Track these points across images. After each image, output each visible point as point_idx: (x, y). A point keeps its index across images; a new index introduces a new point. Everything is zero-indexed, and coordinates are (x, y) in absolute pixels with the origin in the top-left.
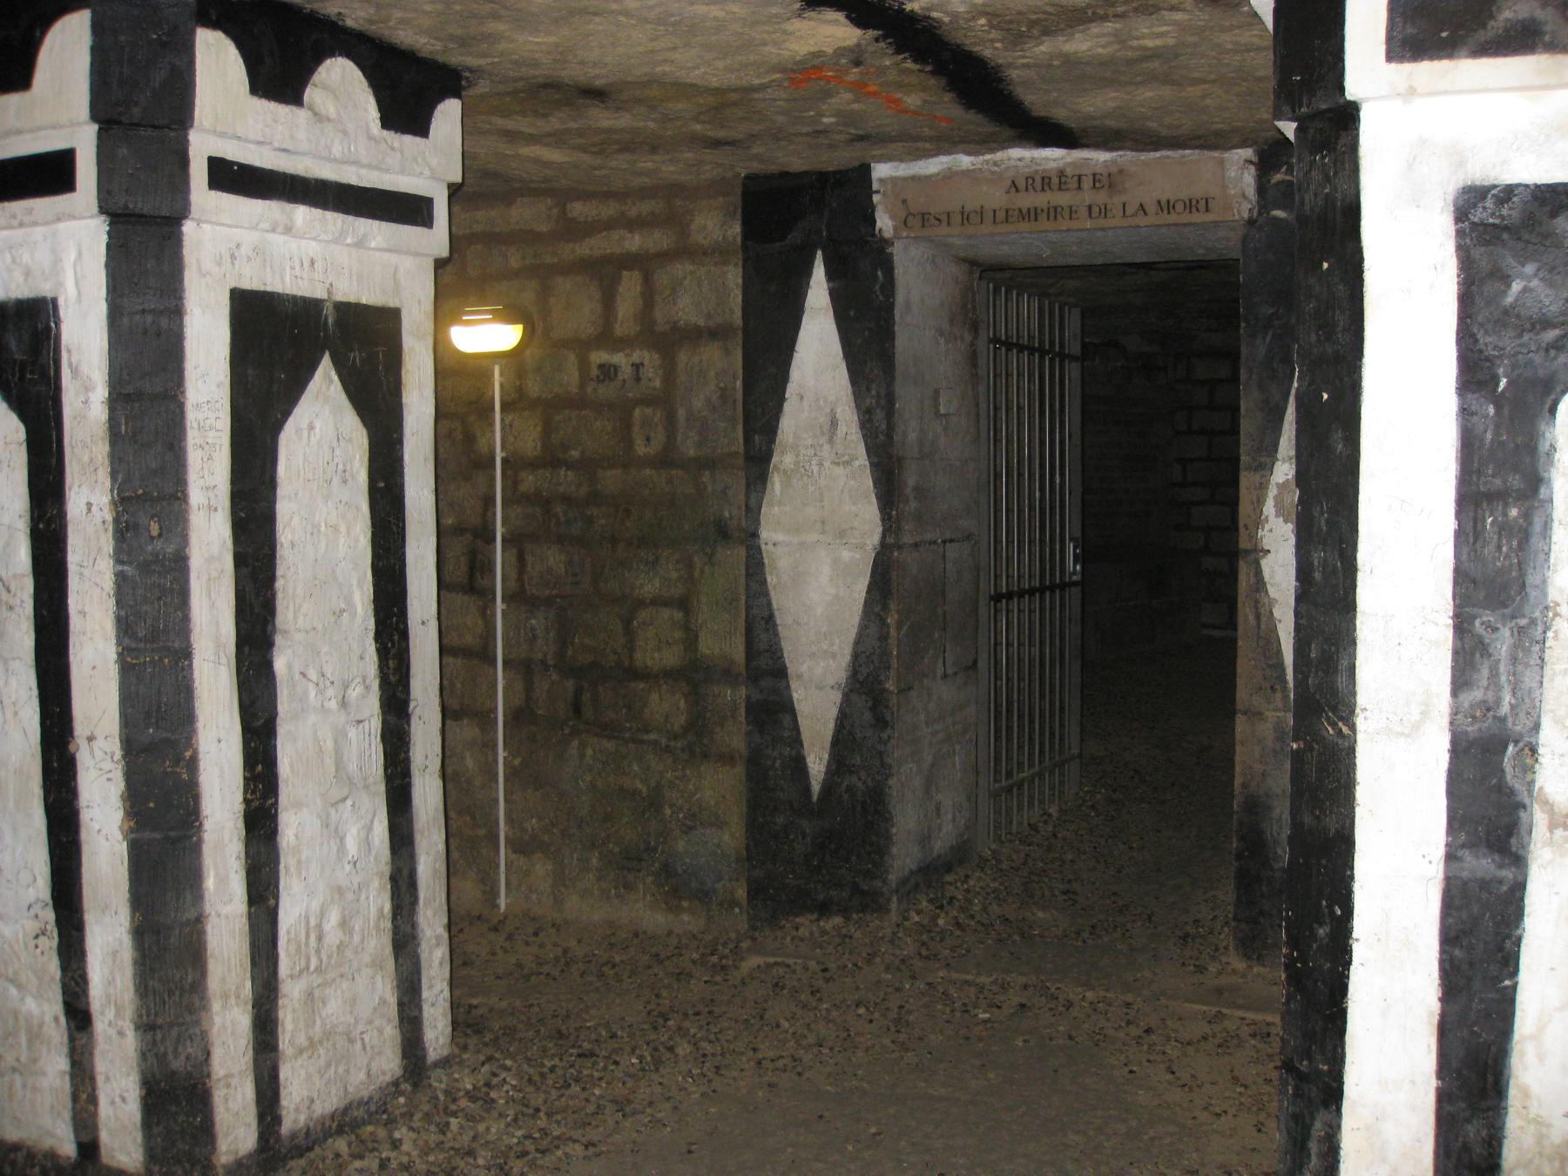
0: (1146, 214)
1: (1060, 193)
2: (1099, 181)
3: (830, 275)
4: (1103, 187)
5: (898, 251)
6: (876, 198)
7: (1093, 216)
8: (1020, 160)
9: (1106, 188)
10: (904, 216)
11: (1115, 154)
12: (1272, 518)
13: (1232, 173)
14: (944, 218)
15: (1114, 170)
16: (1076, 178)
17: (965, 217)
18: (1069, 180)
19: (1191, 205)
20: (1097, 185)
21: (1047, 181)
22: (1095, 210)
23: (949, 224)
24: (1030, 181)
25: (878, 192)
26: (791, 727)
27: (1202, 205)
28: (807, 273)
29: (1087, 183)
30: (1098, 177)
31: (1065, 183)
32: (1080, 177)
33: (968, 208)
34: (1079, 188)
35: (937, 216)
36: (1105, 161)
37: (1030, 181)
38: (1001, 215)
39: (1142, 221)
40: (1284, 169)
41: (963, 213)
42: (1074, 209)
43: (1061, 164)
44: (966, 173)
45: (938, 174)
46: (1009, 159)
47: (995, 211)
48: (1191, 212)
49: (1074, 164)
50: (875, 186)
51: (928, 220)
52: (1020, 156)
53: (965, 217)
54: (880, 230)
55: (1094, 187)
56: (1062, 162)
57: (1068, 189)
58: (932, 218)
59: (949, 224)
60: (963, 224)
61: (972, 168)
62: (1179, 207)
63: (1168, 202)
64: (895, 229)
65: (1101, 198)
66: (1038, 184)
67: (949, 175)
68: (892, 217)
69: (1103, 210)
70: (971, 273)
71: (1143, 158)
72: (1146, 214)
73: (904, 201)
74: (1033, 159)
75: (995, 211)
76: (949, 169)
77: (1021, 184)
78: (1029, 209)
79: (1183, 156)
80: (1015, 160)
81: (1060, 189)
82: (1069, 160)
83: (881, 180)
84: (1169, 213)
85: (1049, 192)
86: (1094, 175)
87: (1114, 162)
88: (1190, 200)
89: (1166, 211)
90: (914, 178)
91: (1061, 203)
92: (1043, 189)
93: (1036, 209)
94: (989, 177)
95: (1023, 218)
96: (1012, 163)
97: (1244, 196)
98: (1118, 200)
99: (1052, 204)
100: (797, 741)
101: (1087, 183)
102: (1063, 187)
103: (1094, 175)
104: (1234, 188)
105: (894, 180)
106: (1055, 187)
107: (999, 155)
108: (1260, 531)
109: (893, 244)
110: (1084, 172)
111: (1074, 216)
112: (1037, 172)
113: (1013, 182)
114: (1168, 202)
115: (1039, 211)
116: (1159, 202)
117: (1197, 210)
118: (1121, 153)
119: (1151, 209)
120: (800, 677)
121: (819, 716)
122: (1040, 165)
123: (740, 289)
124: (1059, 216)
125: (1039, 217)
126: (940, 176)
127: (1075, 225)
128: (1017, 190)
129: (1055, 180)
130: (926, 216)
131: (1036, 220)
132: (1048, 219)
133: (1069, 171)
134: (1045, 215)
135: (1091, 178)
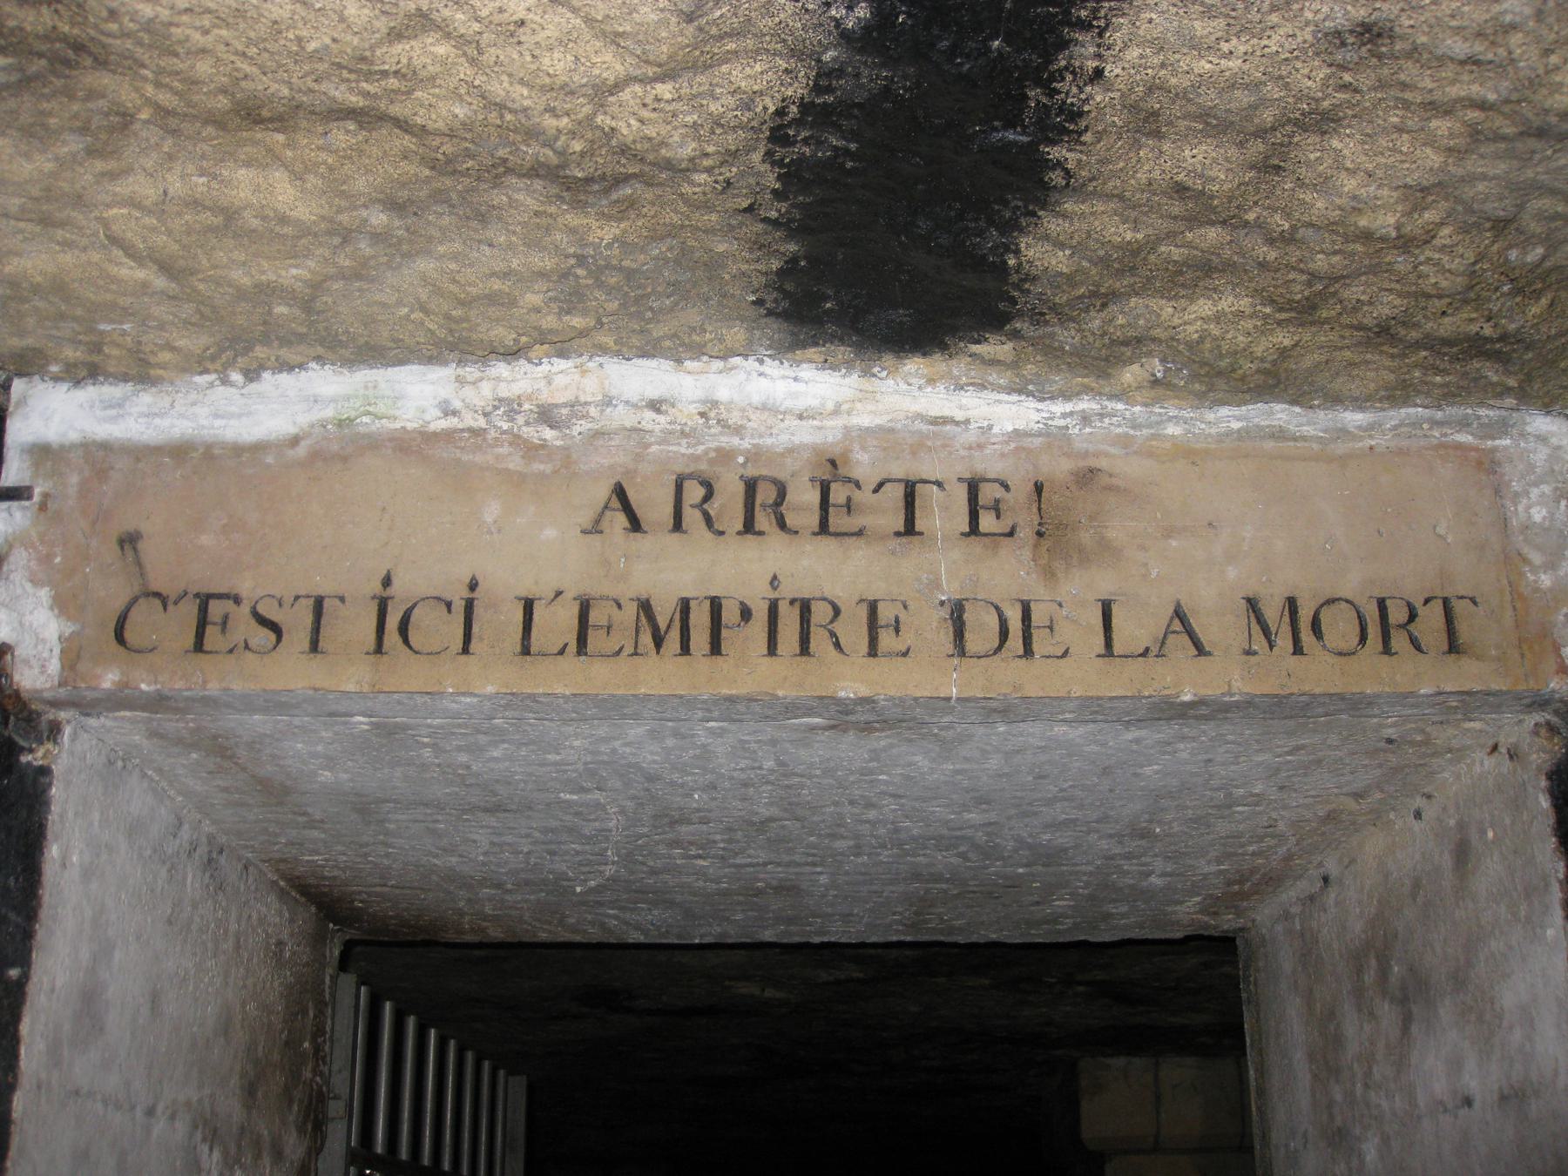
0: (1200, 650)
1: (827, 544)
7: (973, 643)
8: (655, 406)
9: (1025, 533)
10: (119, 604)
11: (1059, 407)
14: (298, 622)
15: (1058, 468)
16: (895, 493)
18: (858, 496)
20: (987, 522)
21: (765, 494)
22: (981, 629)
23: (314, 647)
24: (694, 493)
27: (1431, 622)
30: (988, 493)
31: (849, 506)
34: (910, 529)
37: (694, 493)
38: (556, 623)
42: (886, 614)
43: (828, 434)
45: (295, 441)
46: (608, 401)
47: (528, 606)
48: (1387, 650)
49: (885, 437)
52: (653, 393)
53: (393, 622)
55: (974, 529)
56: (838, 422)
57: (859, 533)
58: (245, 609)
60: (379, 649)
62: (1340, 629)
63: (1292, 604)
64: (72, 654)
68: (62, 605)
70: (319, 939)
71: (1172, 430)
72: (1200, 650)
73: (129, 541)
74: (709, 409)
75: (528, 606)
77: (655, 503)
78: (685, 606)
79: (1343, 433)
81: (824, 528)
82: (864, 419)
83: (42, 453)
84: (1298, 650)
85: (776, 539)
86: (973, 487)
87: (1054, 438)
88: (1382, 604)
89: (1284, 642)
90: (179, 451)
92: (749, 527)
94: (515, 463)
95: (658, 641)
96: (621, 417)
99: (787, 591)
102: (837, 521)
109: (55, 730)
110: (927, 468)
111: (886, 640)
112: (725, 456)
113: (620, 492)
114: (1292, 604)
115: (730, 614)
116: (1252, 604)
117: (1416, 644)
118: (1086, 404)
122: (738, 430)
124: (819, 640)
126: (301, 451)
128: (635, 524)
129: (805, 496)
130: (216, 609)
131: (716, 648)
133: (864, 465)
134: (758, 627)
135: (962, 493)
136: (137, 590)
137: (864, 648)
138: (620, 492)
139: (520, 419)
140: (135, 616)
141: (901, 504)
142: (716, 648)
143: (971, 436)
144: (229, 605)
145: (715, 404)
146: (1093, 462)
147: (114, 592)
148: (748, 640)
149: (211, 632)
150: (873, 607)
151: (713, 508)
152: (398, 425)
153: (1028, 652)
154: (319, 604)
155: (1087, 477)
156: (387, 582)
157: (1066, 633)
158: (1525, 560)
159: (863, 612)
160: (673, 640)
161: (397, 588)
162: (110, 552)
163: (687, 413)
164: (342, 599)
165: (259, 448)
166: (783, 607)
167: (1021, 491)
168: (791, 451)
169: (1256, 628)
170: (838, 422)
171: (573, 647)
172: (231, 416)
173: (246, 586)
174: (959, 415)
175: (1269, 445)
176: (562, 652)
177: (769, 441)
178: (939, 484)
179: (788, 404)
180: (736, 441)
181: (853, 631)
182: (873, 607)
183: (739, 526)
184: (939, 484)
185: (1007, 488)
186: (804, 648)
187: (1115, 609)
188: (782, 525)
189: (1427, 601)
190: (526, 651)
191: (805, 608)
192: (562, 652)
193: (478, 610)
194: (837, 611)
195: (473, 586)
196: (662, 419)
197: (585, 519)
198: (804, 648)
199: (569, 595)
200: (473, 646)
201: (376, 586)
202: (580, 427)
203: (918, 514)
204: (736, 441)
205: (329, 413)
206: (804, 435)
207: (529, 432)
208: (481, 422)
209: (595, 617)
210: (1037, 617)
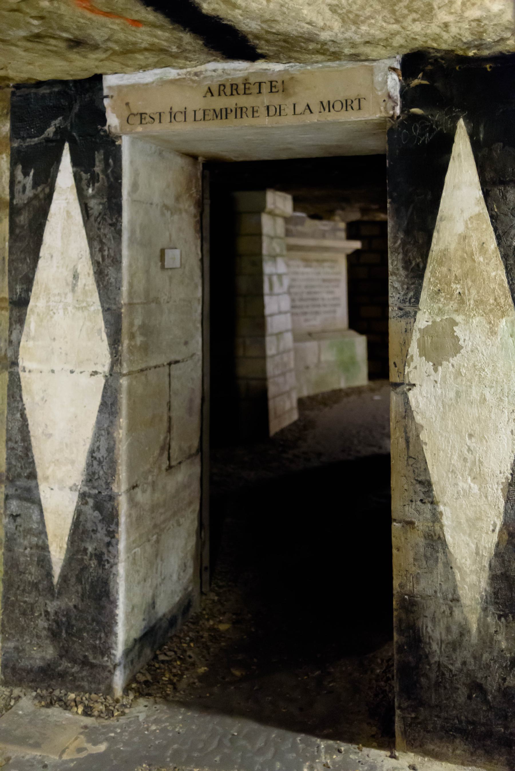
0: (311, 112)
1: (245, 96)
2: (275, 87)
3: (75, 162)
5: (125, 143)
6: (106, 102)
7: (270, 114)
8: (214, 71)
9: (281, 91)
12: (416, 358)
13: (379, 78)
14: (157, 117)
15: (287, 77)
16: (257, 85)
17: (173, 116)
18: (251, 86)
21: (234, 87)
23: (160, 122)
24: (222, 88)
26: (39, 520)
28: (58, 160)
29: (265, 89)
30: (274, 84)
32: (260, 83)
33: (175, 110)
34: (260, 92)
35: (152, 116)
36: (280, 71)
37: (222, 88)
40: (420, 75)
41: (171, 113)
42: (255, 109)
44: (173, 82)
45: (153, 83)
47: (195, 111)
48: (347, 110)
50: (106, 92)
51: (145, 118)
52: (214, 68)
53: (173, 116)
55: (271, 92)
56: (247, 71)
57: (251, 94)
59: (160, 122)
60: (171, 122)
61: (178, 77)
62: (338, 106)
63: (329, 102)
65: (276, 100)
66: (228, 90)
67: (163, 83)
68: (118, 117)
72: (311, 112)
73: (127, 104)
74: (224, 70)
75: (195, 111)
76: (161, 78)
77: (215, 90)
78: (221, 110)
80: (210, 71)
81: (245, 93)
82: (251, 71)
83: (110, 88)
84: (329, 111)
85: (237, 96)
86: (271, 82)
87: (286, 71)
89: (327, 109)
91: (246, 105)
92: (232, 94)
93: (226, 109)
95: (217, 117)
96: (209, 74)
97: (390, 97)
98: (291, 101)
99: (238, 106)
100: (42, 532)
101: (265, 89)
102: (247, 92)
103: (271, 82)
104: (381, 90)
105: (120, 88)
106: (241, 91)
108: (406, 368)
109: (121, 137)
111: (256, 114)
112: (227, 80)
113: (209, 89)
114: (329, 102)
115: (229, 111)
116: (322, 103)
117: (352, 108)
119: (316, 108)
120: (46, 478)
121: (60, 513)
122: (229, 75)
124: (244, 115)
125: (229, 115)
126: (154, 85)
128: (212, 95)
129: (241, 87)
130: (143, 117)
131: (226, 118)
132: (236, 117)
133: (252, 80)
135: (269, 84)
136: (129, 113)
138: (209, 89)
141: (258, 87)
142: (226, 118)
146: (293, 76)
147: (126, 114)
148: (232, 116)
150: (253, 108)
151: (225, 90)
152: (170, 78)
153: (280, 115)
155: (292, 78)
156: (171, 109)
157: (287, 111)
159: (251, 109)
163: (220, 72)
164: (164, 113)
165: (147, 84)
166: (238, 109)
167: (279, 84)
168: (239, 78)
170: (247, 71)
171: (203, 119)
172: (141, 78)
173: (148, 111)
174: (268, 68)
175: (327, 69)
176: (201, 120)
177: (234, 76)
178: (265, 83)
179: (238, 68)
181: (250, 113)
184: (265, 83)
185: (277, 82)
186: (241, 117)
187: (296, 105)
189: (356, 99)
190: (195, 120)
191: (241, 109)
192: (201, 120)
193: (187, 113)
195: (186, 108)
196: (216, 73)
197: (204, 94)
198: (241, 117)
199: (202, 109)
200: (187, 120)
201: (169, 110)
202: (202, 76)
203: (261, 89)
205: (158, 76)
206: (241, 74)
208: (184, 76)
210: (282, 108)
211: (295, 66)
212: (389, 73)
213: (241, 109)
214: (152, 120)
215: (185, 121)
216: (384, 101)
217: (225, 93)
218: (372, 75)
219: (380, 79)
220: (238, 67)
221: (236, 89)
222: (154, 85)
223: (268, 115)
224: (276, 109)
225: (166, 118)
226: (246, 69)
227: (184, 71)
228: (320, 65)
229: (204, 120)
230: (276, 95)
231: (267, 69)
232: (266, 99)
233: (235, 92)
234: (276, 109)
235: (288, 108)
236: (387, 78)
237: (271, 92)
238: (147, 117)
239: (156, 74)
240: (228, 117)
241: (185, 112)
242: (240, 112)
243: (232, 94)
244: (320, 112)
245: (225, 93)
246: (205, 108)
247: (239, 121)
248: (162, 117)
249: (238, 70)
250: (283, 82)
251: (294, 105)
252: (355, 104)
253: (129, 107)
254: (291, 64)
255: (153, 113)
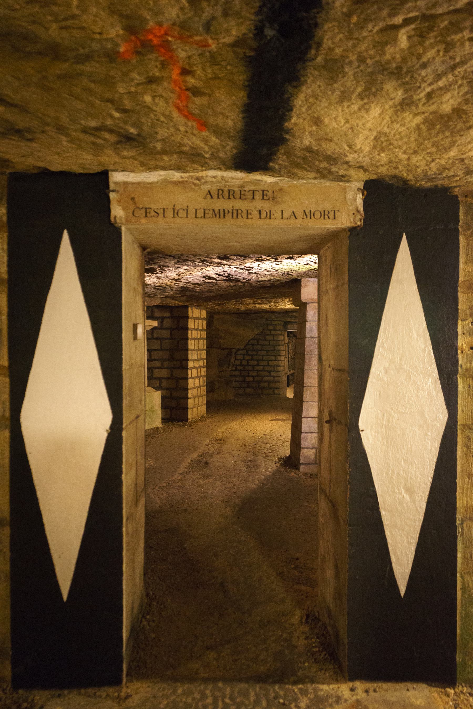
0: (296, 218)
1: (240, 200)
4: (269, 199)
6: (112, 196)
7: (262, 217)
8: (214, 177)
9: (271, 199)
11: (277, 178)
13: (350, 196)
14: (161, 212)
16: (252, 192)
17: (176, 212)
19: (324, 215)
20: (265, 197)
21: (232, 192)
23: (164, 216)
24: (220, 192)
25: (113, 191)
29: (258, 196)
31: (244, 195)
32: (254, 191)
34: (253, 198)
35: (156, 211)
37: (220, 192)
38: (200, 213)
39: (293, 221)
41: (174, 209)
42: (249, 212)
44: (177, 183)
45: (158, 182)
46: (207, 176)
47: (196, 210)
48: (324, 219)
50: (112, 186)
51: (150, 213)
52: (214, 175)
53: (176, 212)
54: (115, 217)
55: (263, 199)
57: (246, 199)
59: (164, 216)
60: (174, 217)
61: (181, 180)
62: (318, 215)
63: (310, 211)
65: (267, 206)
66: (226, 194)
67: (167, 183)
68: (123, 209)
69: (269, 214)
72: (296, 218)
73: (133, 199)
74: (223, 178)
77: (214, 194)
78: (219, 210)
80: (210, 177)
81: (240, 198)
83: (116, 183)
84: (311, 218)
85: (233, 200)
87: (276, 183)
88: (324, 211)
92: (229, 198)
95: (216, 216)
96: (209, 179)
97: (358, 211)
102: (243, 197)
103: (263, 191)
104: (351, 206)
105: (126, 184)
107: (200, 174)
111: (249, 216)
115: (226, 212)
116: (304, 211)
117: (329, 218)
119: (299, 214)
123: (6, 252)
124: (240, 216)
125: (226, 216)
127: (250, 222)
128: (212, 197)
130: (148, 210)
131: (224, 217)
132: (233, 217)
135: (261, 192)
137: (246, 217)
138: (209, 192)
139: (193, 179)
140: (135, 211)
141: (252, 195)
142: (224, 217)
143: (263, 183)
144: (150, 210)
145: (223, 177)
147: (132, 207)
148: (229, 216)
149: (148, 214)
150: (247, 211)
153: (270, 218)
154: (164, 209)
155: (281, 190)
156: (174, 206)
158: (348, 205)
159: (246, 212)
160: (218, 216)
161: (176, 207)
162: (130, 202)
163: (219, 179)
165: (152, 183)
167: (270, 193)
169: (304, 215)
171: (203, 217)
172: (147, 178)
173: (153, 206)
174: (261, 179)
175: (309, 185)
178: (258, 191)
180: (227, 183)
181: (244, 215)
182: (247, 211)
183: (228, 197)
184: (258, 191)
185: (268, 191)
186: (237, 217)
188: (234, 197)
190: (196, 217)
192: (201, 217)
193: (189, 211)
194: (242, 211)
195: (187, 207)
197: (204, 196)
198: (237, 217)
200: (189, 216)
201: (172, 207)
202: (203, 181)
204: (227, 183)
205: (163, 177)
206: (238, 182)
207: (195, 182)
208: (187, 179)
209: (207, 211)
211: (284, 180)
212: (357, 192)
213: (237, 211)
214: (156, 214)
215: (187, 217)
216: (354, 214)
217: (223, 197)
218: (345, 193)
219: (351, 197)
220: (236, 176)
221: (233, 195)
222: (159, 184)
223: (260, 218)
224: (267, 213)
225: (169, 213)
226: (242, 179)
227: (187, 175)
228: (305, 181)
229: (204, 217)
230: (268, 202)
231: (259, 180)
232: (258, 204)
233: (231, 197)
234: (267, 213)
235: (277, 213)
236: (356, 197)
237: (263, 199)
238: (152, 211)
239: (161, 175)
240: (226, 217)
241: (187, 210)
242: (236, 214)
243: (229, 198)
244: (303, 219)
245: (223, 197)
246: (205, 208)
247: (235, 221)
248: (165, 212)
249: (235, 179)
250: (273, 192)
251: (282, 211)
252: (331, 215)
253: (135, 203)
254: (281, 178)
255: (158, 209)
